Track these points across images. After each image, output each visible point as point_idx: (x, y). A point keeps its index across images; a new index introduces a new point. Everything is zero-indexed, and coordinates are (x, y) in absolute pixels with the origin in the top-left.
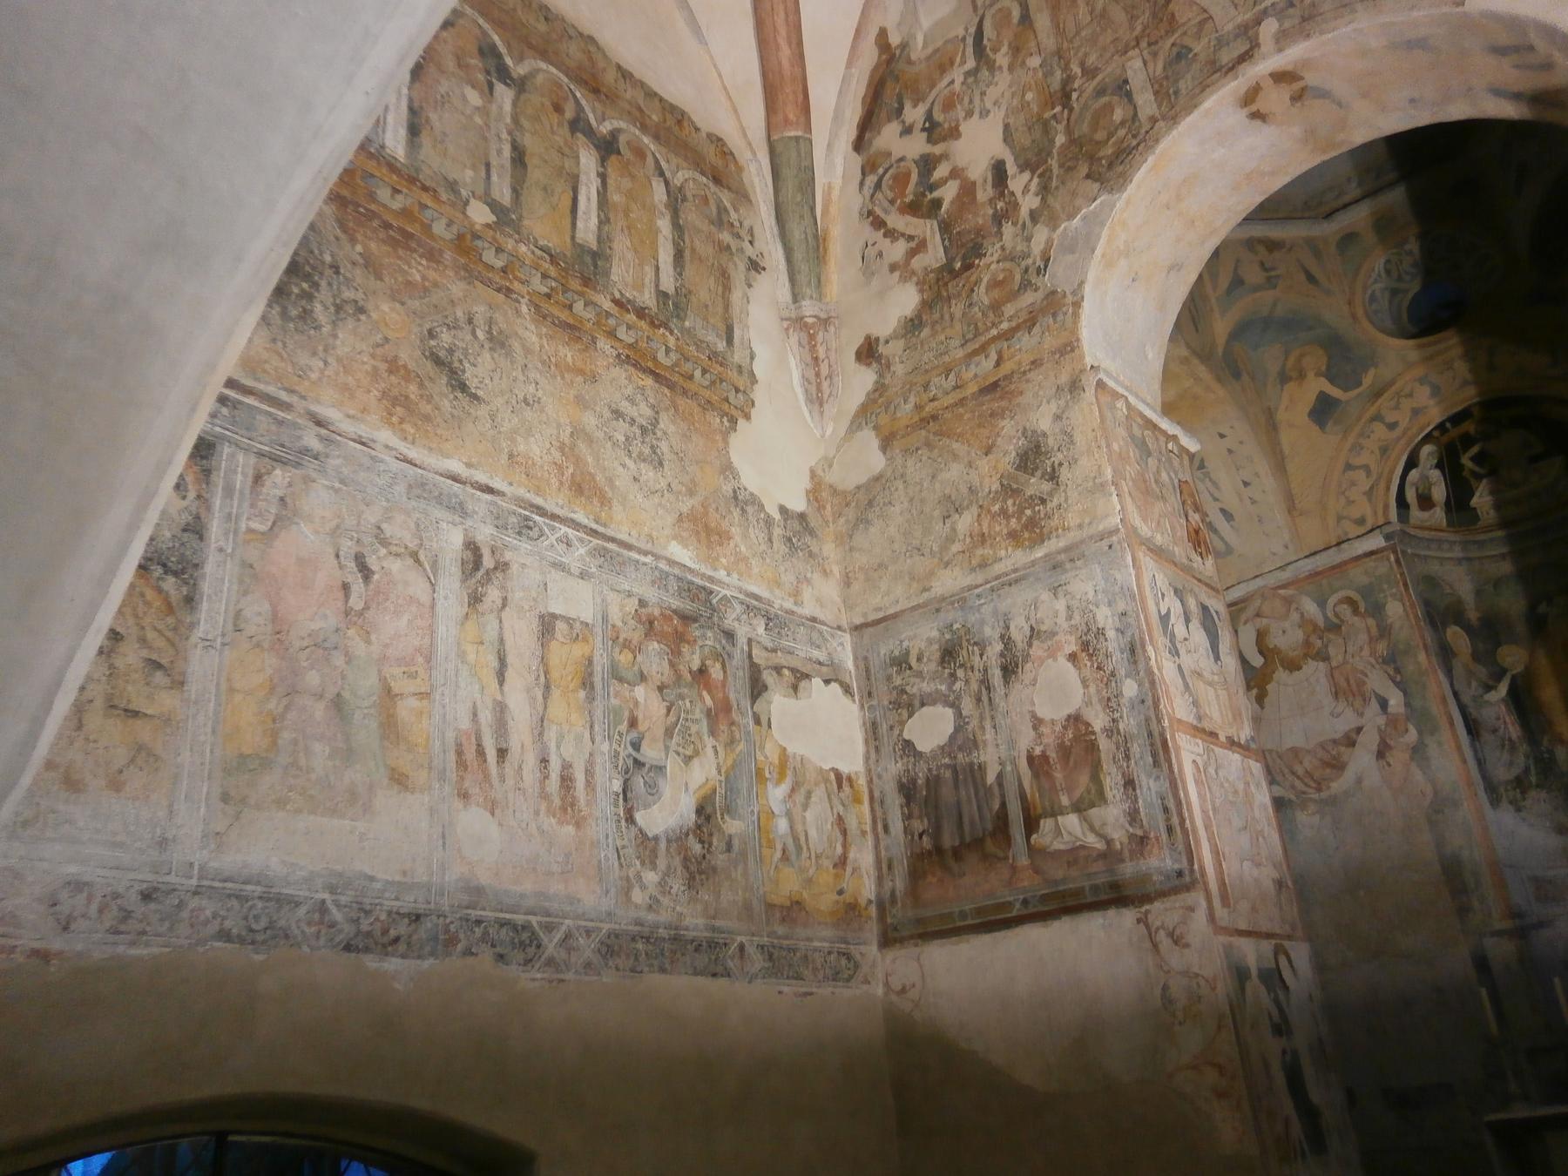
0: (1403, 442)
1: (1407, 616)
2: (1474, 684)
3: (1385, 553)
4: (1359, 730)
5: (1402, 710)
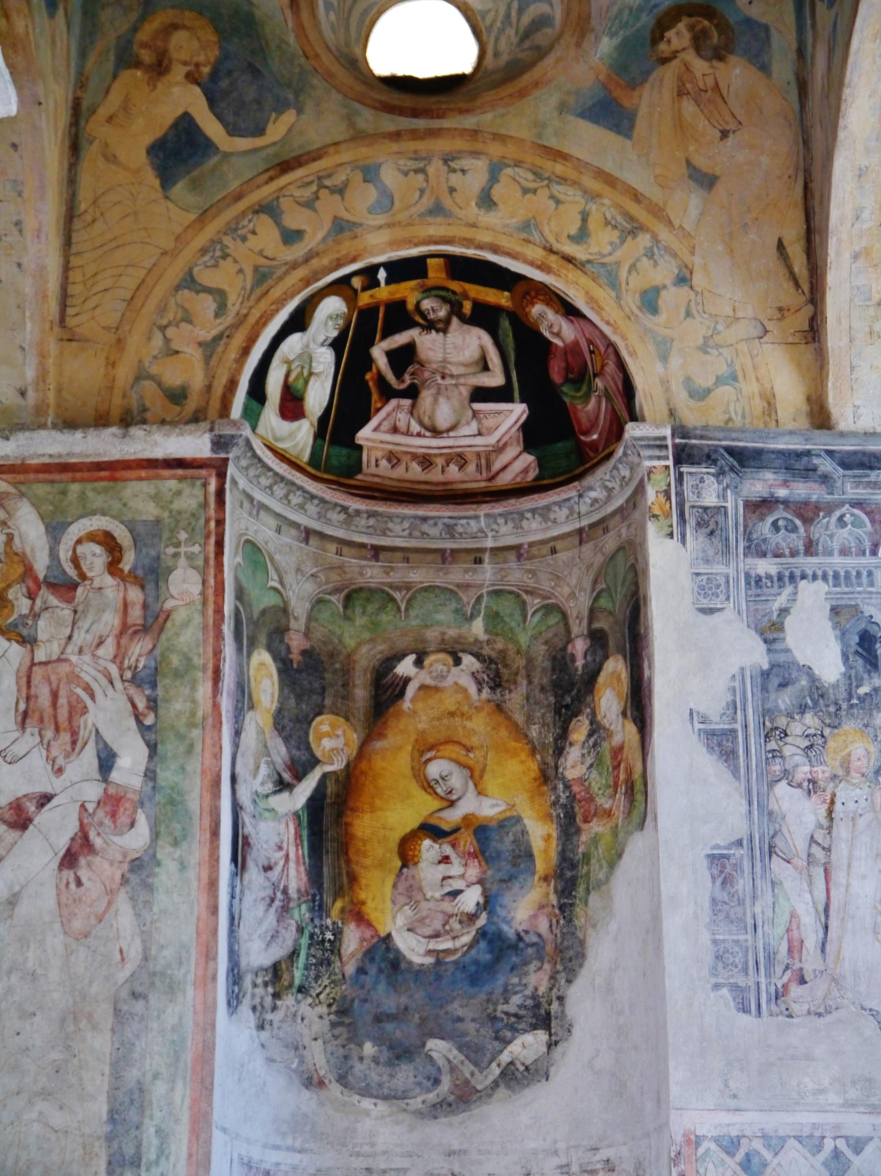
0: (301, 272)
1: (205, 603)
2: (264, 770)
3: (203, 472)
4: (45, 799)
5: (137, 782)
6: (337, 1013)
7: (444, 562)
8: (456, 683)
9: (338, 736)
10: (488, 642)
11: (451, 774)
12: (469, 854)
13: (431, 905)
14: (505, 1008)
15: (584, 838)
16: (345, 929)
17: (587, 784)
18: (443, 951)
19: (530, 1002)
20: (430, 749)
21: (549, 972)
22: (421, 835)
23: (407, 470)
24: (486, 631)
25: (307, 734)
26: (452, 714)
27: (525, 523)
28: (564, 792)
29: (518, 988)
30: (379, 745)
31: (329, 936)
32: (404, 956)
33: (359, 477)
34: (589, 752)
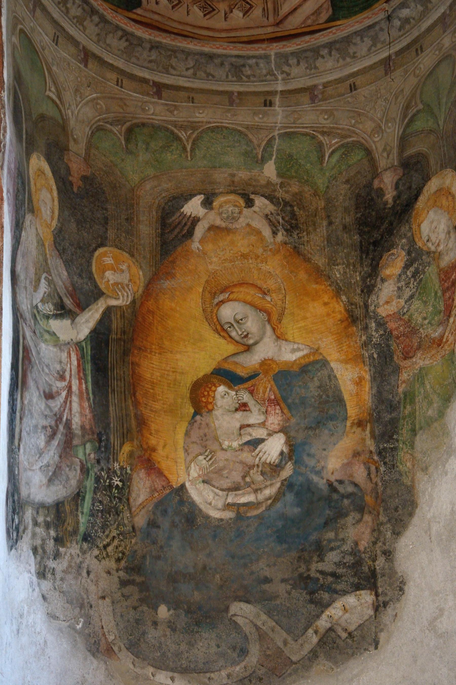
2: (43, 287)
6: (127, 569)
7: (231, 104)
8: (248, 225)
9: (122, 271)
10: (282, 185)
11: (246, 317)
12: (269, 400)
13: (228, 455)
14: (321, 566)
15: (404, 376)
16: (135, 476)
17: (406, 317)
18: (244, 505)
19: (349, 559)
20: (223, 291)
21: (370, 524)
22: (215, 381)
23: (188, 14)
24: (279, 175)
25: (89, 263)
26: (244, 256)
27: (319, 63)
28: (376, 331)
29: (332, 545)
30: (167, 284)
31: (117, 482)
32: (200, 510)
33: (139, 11)
34: (407, 285)
